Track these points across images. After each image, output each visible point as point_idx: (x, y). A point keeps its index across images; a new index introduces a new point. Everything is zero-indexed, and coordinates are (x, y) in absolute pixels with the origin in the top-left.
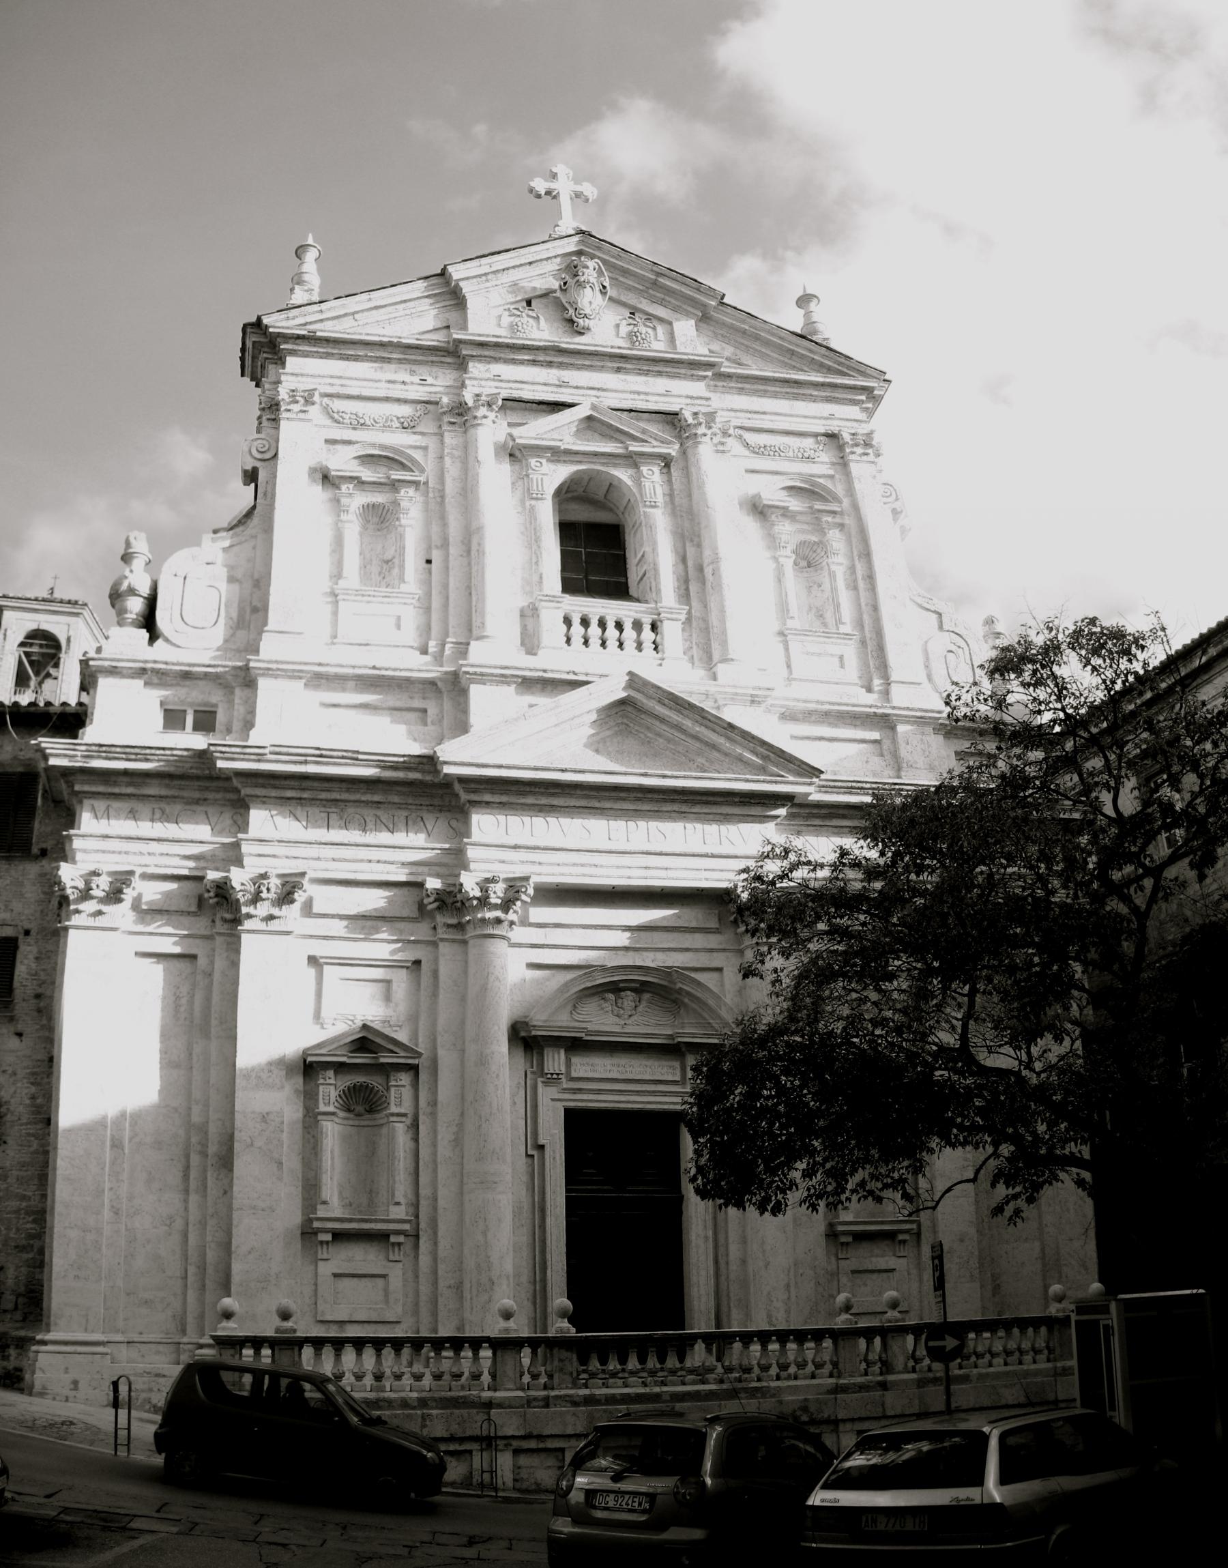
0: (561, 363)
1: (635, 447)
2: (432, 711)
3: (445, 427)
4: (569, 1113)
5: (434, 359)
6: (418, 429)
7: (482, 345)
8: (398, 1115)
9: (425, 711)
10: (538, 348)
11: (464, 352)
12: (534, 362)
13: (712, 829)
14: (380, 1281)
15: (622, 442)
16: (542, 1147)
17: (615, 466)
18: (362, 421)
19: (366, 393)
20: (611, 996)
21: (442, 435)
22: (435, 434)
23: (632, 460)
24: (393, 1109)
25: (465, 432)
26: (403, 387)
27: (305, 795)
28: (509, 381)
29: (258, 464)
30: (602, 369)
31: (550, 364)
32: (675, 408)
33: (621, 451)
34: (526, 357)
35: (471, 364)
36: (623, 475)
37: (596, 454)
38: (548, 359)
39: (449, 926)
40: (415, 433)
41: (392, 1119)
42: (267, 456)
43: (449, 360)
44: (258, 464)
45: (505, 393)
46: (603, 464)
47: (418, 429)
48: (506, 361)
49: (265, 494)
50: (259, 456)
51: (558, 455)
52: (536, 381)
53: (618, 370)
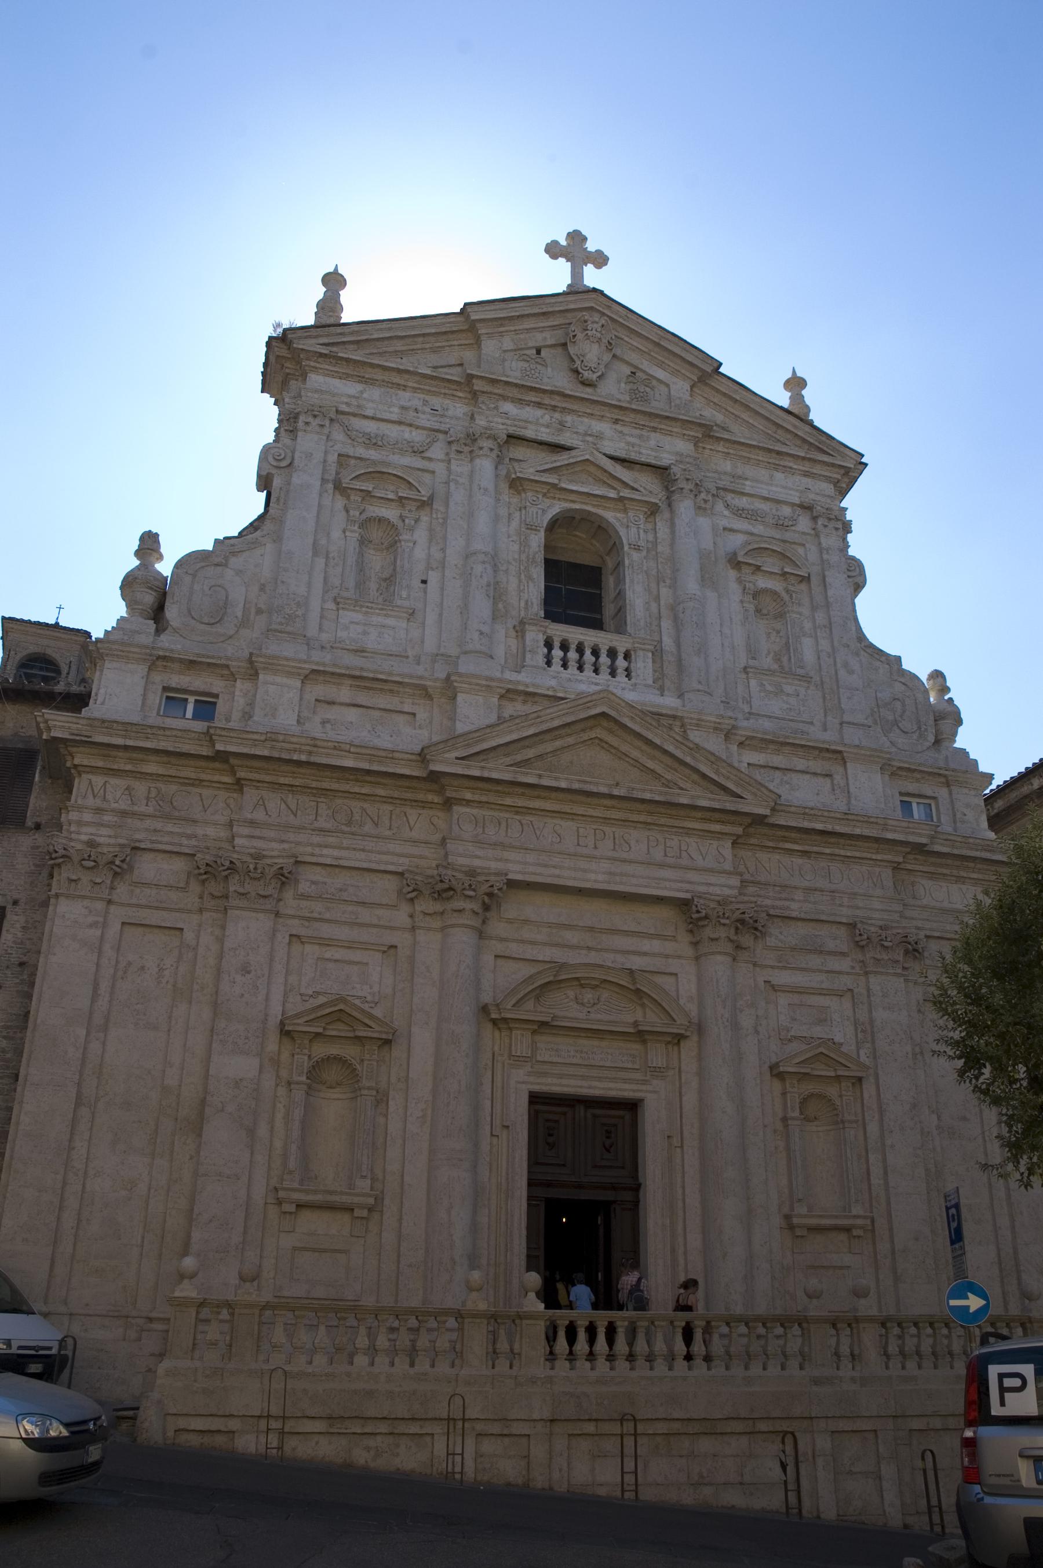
0: (564, 408)
1: (626, 493)
2: (422, 715)
3: (453, 455)
4: (535, 1099)
6: (427, 454)
8: (369, 1088)
9: (414, 714)
10: (544, 391)
12: (539, 405)
15: (615, 489)
18: (374, 441)
19: (379, 416)
21: (449, 461)
22: (443, 461)
24: (365, 1083)
25: (472, 460)
29: (274, 471)
31: (554, 408)
32: (665, 462)
34: (533, 399)
35: (480, 399)
36: (610, 516)
38: (553, 403)
40: (423, 458)
41: (365, 1092)
42: (284, 464)
44: (274, 471)
45: (512, 430)
46: (594, 506)
47: (427, 454)
48: (514, 400)
49: (278, 499)
50: (275, 464)
52: (537, 423)
53: (616, 421)
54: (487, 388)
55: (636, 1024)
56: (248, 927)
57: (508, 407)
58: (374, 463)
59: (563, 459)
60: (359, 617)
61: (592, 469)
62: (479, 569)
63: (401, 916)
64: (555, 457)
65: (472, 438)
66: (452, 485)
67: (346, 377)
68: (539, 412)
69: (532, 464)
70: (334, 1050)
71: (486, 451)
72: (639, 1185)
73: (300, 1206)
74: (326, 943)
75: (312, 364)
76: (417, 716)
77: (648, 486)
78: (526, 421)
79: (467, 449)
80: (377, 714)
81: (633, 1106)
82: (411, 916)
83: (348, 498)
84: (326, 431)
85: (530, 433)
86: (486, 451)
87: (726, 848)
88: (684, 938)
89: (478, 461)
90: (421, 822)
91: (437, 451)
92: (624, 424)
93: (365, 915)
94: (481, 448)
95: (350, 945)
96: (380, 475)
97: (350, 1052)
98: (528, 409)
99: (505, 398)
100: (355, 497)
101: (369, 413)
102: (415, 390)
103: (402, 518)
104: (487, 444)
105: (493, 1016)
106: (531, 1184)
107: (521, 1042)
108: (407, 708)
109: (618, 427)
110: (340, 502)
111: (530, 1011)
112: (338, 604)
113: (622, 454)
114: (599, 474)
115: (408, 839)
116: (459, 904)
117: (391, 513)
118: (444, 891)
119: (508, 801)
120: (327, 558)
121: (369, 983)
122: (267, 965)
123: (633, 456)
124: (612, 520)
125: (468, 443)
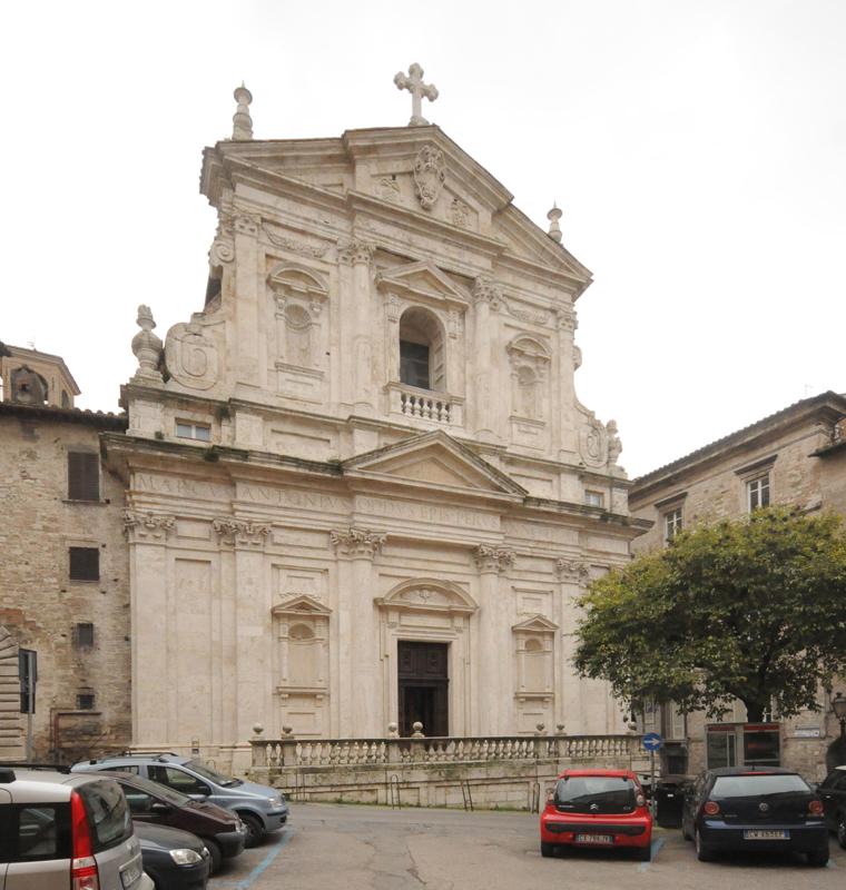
5: (333, 207)
7: (366, 203)
11: (355, 206)
12: (396, 224)
13: (471, 516)
14: (312, 716)
16: (387, 656)
17: (435, 307)
20: (418, 592)
23: (446, 305)
26: (313, 224)
27: (268, 480)
28: (381, 235)
30: (435, 238)
31: (405, 228)
33: (441, 298)
35: (357, 216)
36: (438, 312)
37: (427, 297)
39: (343, 553)
43: (344, 211)
51: (405, 293)
53: (444, 241)
54: (362, 208)
55: (449, 607)
56: (249, 562)
57: (376, 225)
58: (292, 264)
59: (410, 269)
60: (291, 377)
61: (429, 278)
62: (362, 346)
63: (330, 555)
64: (406, 266)
65: (353, 249)
66: (342, 284)
67: (264, 189)
68: (396, 230)
69: (394, 273)
70: (301, 622)
71: (363, 260)
72: (448, 681)
73: (290, 694)
74: (290, 568)
75: (240, 175)
76: (332, 442)
77: (461, 294)
78: (388, 237)
79: (350, 258)
80: (307, 440)
81: (443, 648)
82: (335, 554)
83: (275, 290)
84: (256, 234)
85: (390, 247)
86: (363, 260)
87: (498, 520)
88: (473, 566)
89: (357, 267)
90: (336, 505)
91: (330, 257)
92: (450, 243)
93: (312, 554)
94: (360, 257)
95: (304, 569)
96: (297, 275)
97: (309, 623)
98: (389, 226)
99: (373, 216)
100: (281, 292)
101: (283, 221)
102: (314, 205)
103: (312, 308)
104: (364, 254)
105: (380, 604)
106: (400, 681)
107: (394, 617)
108: (324, 437)
109: (446, 246)
110: (271, 294)
111: (398, 602)
112: (277, 367)
113: (447, 267)
114: (432, 281)
115: (327, 511)
116: (362, 549)
117: (304, 304)
118: (354, 542)
119: (386, 493)
120: (267, 334)
121: (315, 589)
122: (259, 582)
123: (455, 269)
124: (440, 316)
125: (350, 254)
